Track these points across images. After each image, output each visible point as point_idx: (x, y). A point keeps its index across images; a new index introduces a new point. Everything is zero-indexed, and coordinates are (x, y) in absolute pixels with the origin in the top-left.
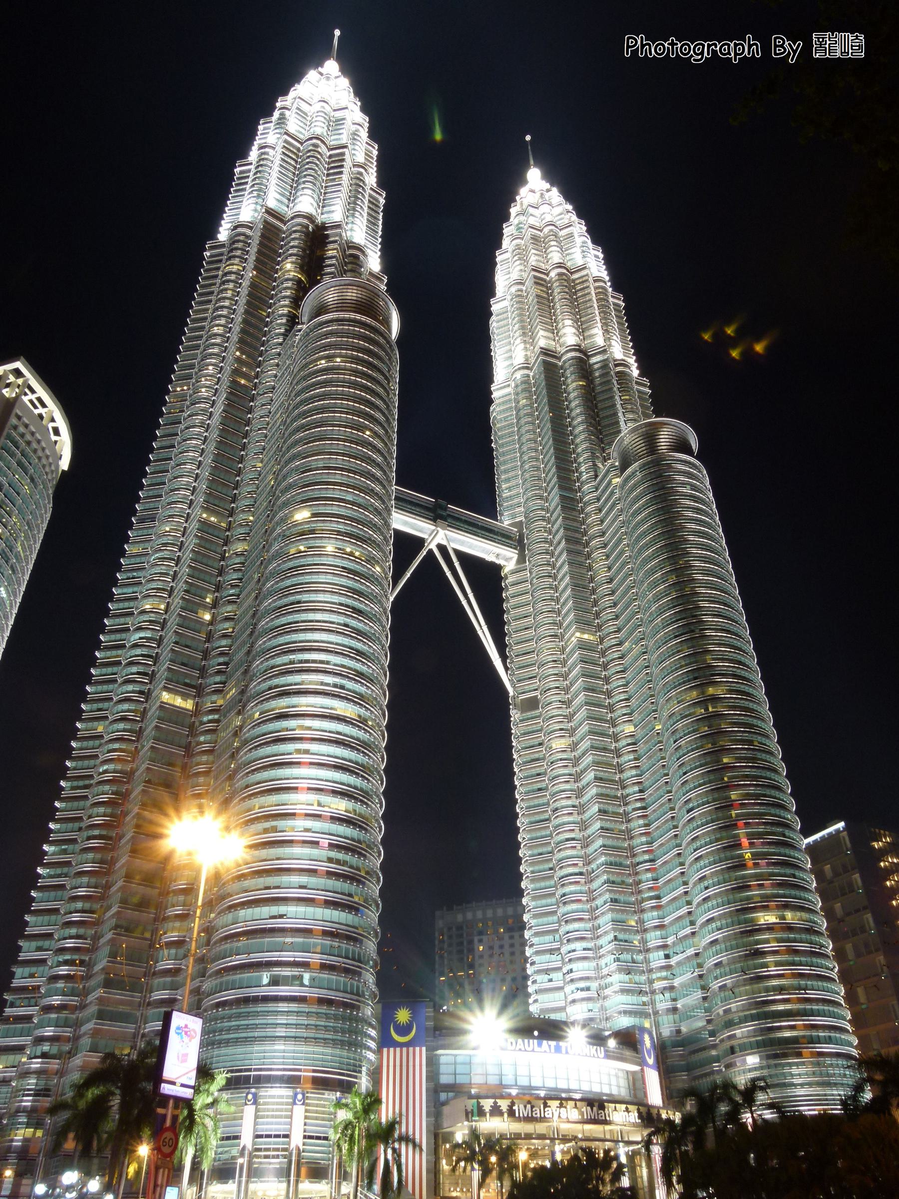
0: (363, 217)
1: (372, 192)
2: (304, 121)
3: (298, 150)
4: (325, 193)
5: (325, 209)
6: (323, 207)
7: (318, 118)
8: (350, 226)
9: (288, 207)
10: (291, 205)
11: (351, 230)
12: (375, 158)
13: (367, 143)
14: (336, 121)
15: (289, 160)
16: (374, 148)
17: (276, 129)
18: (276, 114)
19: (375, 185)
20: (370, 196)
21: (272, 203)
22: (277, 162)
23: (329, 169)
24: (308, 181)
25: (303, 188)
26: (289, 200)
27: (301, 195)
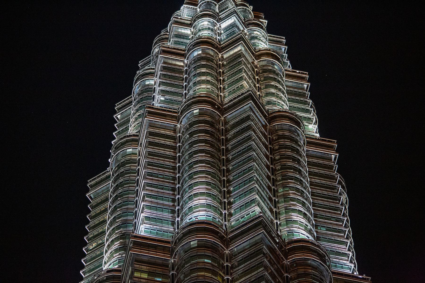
1: (313, 149)
5: (235, 206)
6: (230, 203)
8: (283, 217)
9: (173, 224)
11: (289, 222)
13: (288, 76)
14: (228, 63)
15: (161, 151)
16: (303, 78)
17: (137, 110)
18: (136, 89)
19: (318, 135)
24: (196, 173)
25: (191, 187)
26: (173, 212)
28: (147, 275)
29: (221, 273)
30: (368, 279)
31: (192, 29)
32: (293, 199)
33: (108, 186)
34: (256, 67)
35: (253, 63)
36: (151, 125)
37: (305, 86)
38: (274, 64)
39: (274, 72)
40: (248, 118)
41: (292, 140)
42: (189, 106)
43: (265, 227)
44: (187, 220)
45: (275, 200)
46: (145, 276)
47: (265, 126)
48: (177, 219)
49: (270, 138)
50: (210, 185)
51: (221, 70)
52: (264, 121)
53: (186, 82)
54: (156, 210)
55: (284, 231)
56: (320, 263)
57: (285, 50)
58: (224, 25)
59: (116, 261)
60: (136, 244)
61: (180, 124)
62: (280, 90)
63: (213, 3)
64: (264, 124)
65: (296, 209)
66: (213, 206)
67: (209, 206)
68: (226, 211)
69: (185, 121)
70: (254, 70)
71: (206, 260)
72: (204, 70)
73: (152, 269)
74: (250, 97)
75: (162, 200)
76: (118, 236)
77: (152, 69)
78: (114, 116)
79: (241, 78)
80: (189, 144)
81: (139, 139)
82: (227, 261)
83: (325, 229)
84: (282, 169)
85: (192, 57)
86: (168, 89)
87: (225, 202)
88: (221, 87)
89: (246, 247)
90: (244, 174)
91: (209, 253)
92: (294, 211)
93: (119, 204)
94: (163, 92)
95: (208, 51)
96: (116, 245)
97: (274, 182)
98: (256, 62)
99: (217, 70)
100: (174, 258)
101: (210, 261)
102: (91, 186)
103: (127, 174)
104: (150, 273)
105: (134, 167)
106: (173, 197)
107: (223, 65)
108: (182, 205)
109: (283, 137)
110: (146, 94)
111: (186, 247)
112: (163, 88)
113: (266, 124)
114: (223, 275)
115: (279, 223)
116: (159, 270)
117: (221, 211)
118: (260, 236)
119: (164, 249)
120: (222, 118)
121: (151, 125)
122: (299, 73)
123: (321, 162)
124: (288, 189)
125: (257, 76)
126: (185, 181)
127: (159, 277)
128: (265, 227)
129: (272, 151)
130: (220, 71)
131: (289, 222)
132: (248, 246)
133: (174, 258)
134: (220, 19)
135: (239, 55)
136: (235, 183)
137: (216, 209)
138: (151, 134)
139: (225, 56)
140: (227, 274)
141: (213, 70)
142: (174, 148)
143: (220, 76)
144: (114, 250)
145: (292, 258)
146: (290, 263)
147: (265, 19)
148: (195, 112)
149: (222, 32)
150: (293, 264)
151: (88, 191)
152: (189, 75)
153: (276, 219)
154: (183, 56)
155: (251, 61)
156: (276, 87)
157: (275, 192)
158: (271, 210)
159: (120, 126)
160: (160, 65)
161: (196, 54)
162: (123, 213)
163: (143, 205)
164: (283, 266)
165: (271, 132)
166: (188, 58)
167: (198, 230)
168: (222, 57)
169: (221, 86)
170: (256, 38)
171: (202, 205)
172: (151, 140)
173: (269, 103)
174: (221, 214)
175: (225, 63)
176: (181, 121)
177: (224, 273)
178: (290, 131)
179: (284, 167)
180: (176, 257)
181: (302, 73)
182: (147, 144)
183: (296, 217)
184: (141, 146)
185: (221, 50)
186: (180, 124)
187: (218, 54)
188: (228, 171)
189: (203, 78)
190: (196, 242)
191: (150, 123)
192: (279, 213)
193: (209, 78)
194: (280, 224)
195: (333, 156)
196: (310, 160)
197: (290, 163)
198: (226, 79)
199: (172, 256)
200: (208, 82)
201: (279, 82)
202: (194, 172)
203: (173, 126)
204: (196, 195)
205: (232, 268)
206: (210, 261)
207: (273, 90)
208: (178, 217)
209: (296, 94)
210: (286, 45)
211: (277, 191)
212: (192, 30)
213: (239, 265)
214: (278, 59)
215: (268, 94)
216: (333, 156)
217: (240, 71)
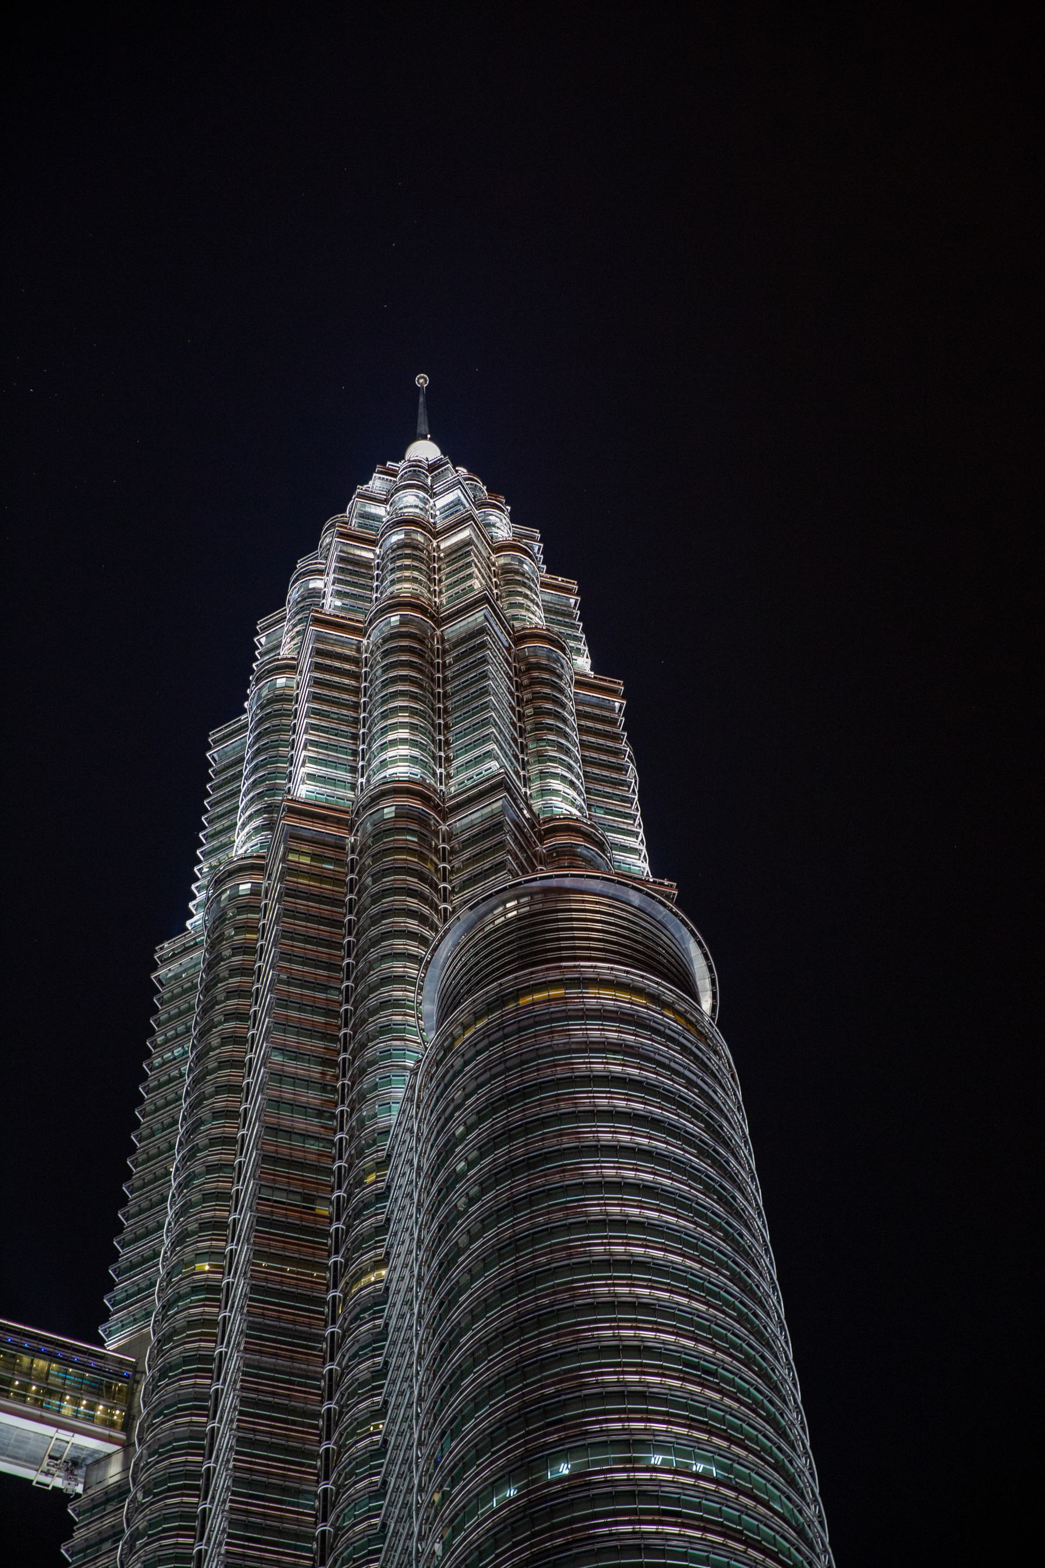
2: (362, 581)
5: (456, 763)
6: (448, 760)
7: (398, 563)
8: (536, 785)
9: (353, 787)
11: (544, 792)
12: (577, 612)
13: (544, 585)
16: (569, 591)
18: (294, 594)
21: (303, 791)
25: (384, 731)
26: (353, 770)
28: (309, 859)
29: (434, 859)
30: (672, 886)
31: (388, 506)
32: (553, 759)
33: (242, 740)
34: (494, 565)
35: (488, 558)
37: (572, 601)
38: (521, 562)
39: (523, 574)
40: (482, 631)
41: (552, 671)
42: (382, 611)
43: (508, 790)
44: (376, 779)
45: (523, 759)
46: (306, 860)
47: (509, 649)
48: (360, 780)
49: (515, 667)
50: (417, 728)
51: (436, 565)
52: (507, 641)
53: (377, 580)
54: (326, 766)
55: (537, 804)
56: (597, 853)
57: (539, 549)
58: (442, 502)
59: (257, 844)
60: (291, 811)
61: (368, 639)
62: (532, 601)
63: (423, 473)
64: (507, 645)
65: (558, 774)
66: (421, 760)
67: (414, 760)
68: (443, 770)
69: (375, 635)
70: (489, 569)
71: (409, 838)
72: (407, 562)
73: (318, 850)
74: (484, 599)
75: (336, 751)
76: (261, 808)
77: (320, 563)
78: (255, 640)
79: (470, 576)
80: (383, 667)
81: (298, 664)
82: (444, 841)
83: (602, 812)
84: (535, 714)
85: (388, 544)
86: (348, 589)
87: (440, 757)
88: (435, 590)
89: (475, 822)
90: (474, 714)
91: (414, 826)
92: (555, 776)
93: (262, 761)
94: (339, 594)
95: (414, 536)
97: (522, 732)
98: (493, 557)
99: (429, 565)
100: (355, 835)
101: (415, 840)
102: (215, 742)
103: (276, 716)
104: (314, 857)
106: (354, 747)
107: (440, 559)
108: (369, 759)
109: (539, 667)
110: (309, 601)
111: (375, 817)
112: (338, 587)
113: (510, 645)
114: (437, 861)
115: (529, 793)
116: (329, 853)
117: (433, 769)
118: (500, 803)
119: (338, 822)
120: (438, 632)
121: (319, 638)
122: (562, 581)
123: (597, 712)
124: (544, 744)
125: (495, 577)
126: (373, 724)
127: (330, 863)
128: (508, 790)
129: (519, 687)
130: (434, 567)
131: (544, 792)
132: (480, 820)
133: (355, 835)
134: (435, 494)
135: (468, 542)
136: (456, 729)
137: (424, 765)
138: (319, 652)
139: (443, 546)
140: (444, 860)
141: (423, 563)
142: (356, 676)
143: (435, 574)
144: (253, 829)
145: (551, 842)
146: (547, 851)
147: (507, 503)
148: (393, 619)
149: (438, 513)
150: (552, 854)
151: (209, 748)
152: (382, 570)
153: (525, 786)
154: (374, 543)
155: (485, 555)
156: (526, 596)
157: (523, 748)
158: (517, 773)
159: (262, 654)
160: (334, 553)
161: (395, 538)
162: (268, 774)
163: (306, 739)
164: (535, 854)
165: (516, 658)
166: (381, 546)
167: (396, 792)
168: (438, 546)
169: (436, 588)
170: (494, 525)
171: (404, 759)
172: (319, 660)
173: (515, 618)
174: (434, 774)
175: (442, 555)
176: (370, 636)
177: (439, 859)
178: (548, 658)
179: (539, 712)
180: (359, 834)
181: (567, 582)
182: (313, 668)
183: (556, 784)
184: (300, 674)
185: (436, 535)
186: (368, 639)
187: (431, 541)
188: (446, 711)
189: (407, 574)
190: (393, 808)
191: (317, 636)
192: (529, 779)
193: (416, 574)
194: (531, 795)
195: (617, 704)
196: (580, 708)
198: (444, 578)
199: (352, 832)
200: (415, 580)
201: (530, 589)
202: (390, 708)
203: (356, 642)
204: (393, 743)
205: (453, 852)
206: (415, 840)
207: (520, 600)
208: (362, 776)
209: (557, 613)
210: (540, 542)
211: (526, 746)
212: (388, 509)
213: (464, 848)
214: (530, 557)
215: (512, 605)
216: (617, 704)
217: (468, 565)
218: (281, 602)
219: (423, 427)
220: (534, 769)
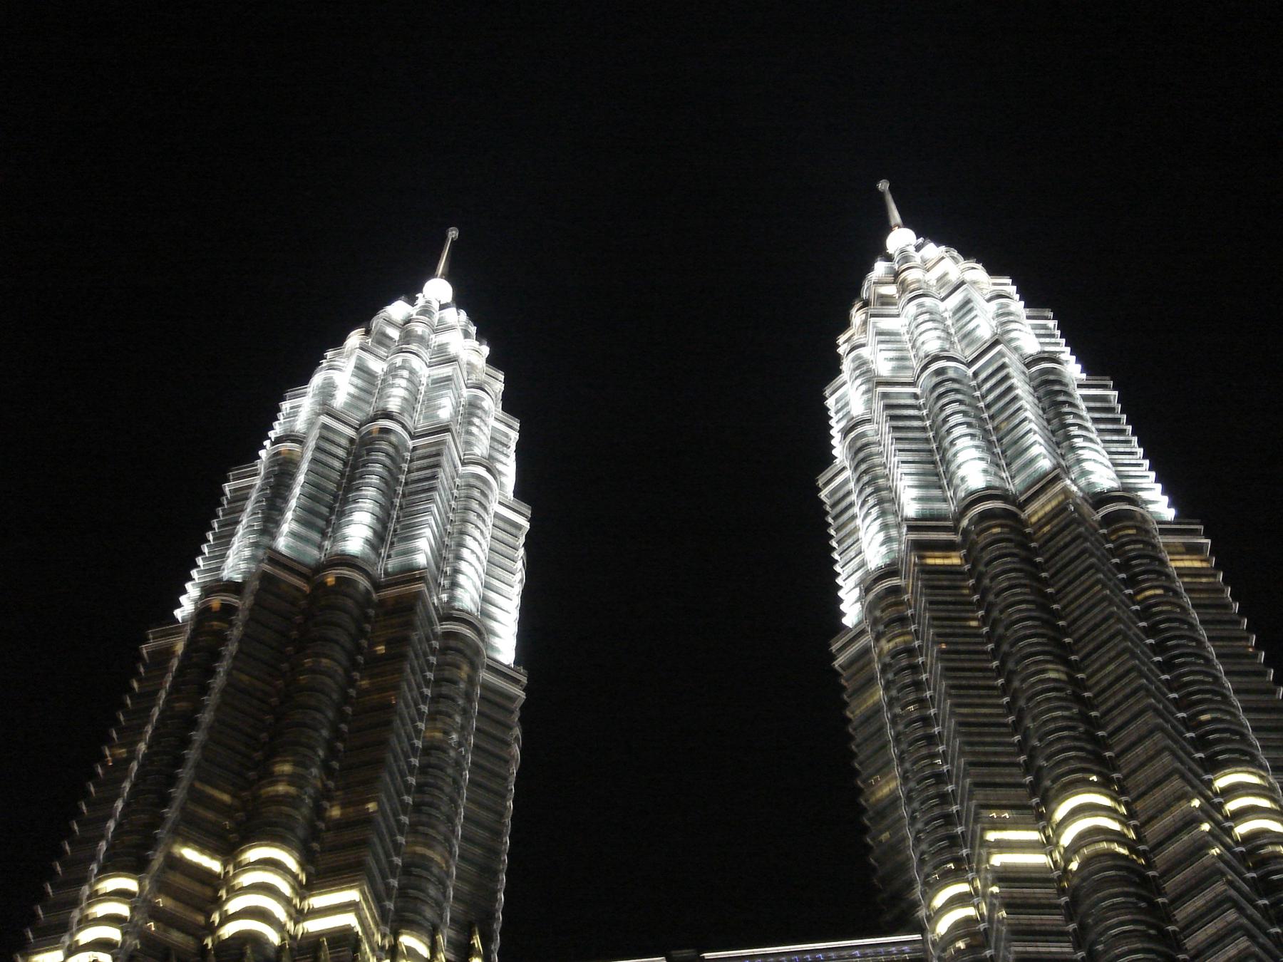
0: (1091, 440)
2: (899, 346)
3: (915, 396)
4: (999, 440)
5: (1014, 467)
7: (923, 327)
8: (1076, 470)
9: (945, 500)
10: (949, 494)
11: (1084, 473)
12: (1058, 333)
13: (1028, 318)
16: (1046, 318)
19: (1084, 376)
20: (1085, 398)
21: (911, 509)
22: (888, 438)
23: (984, 397)
26: (941, 487)
27: (959, 467)
36: (885, 395)
47: (1024, 373)
96: (881, 536)
105: (874, 449)
154: (898, 316)
197: (1066, 409)
218: (840, 372)
219: (895, 216)
220: (1071, 457)
